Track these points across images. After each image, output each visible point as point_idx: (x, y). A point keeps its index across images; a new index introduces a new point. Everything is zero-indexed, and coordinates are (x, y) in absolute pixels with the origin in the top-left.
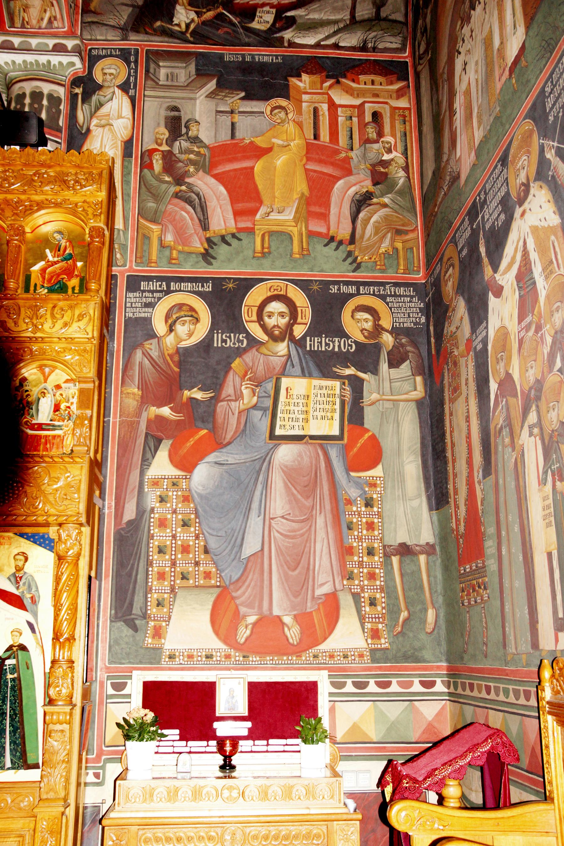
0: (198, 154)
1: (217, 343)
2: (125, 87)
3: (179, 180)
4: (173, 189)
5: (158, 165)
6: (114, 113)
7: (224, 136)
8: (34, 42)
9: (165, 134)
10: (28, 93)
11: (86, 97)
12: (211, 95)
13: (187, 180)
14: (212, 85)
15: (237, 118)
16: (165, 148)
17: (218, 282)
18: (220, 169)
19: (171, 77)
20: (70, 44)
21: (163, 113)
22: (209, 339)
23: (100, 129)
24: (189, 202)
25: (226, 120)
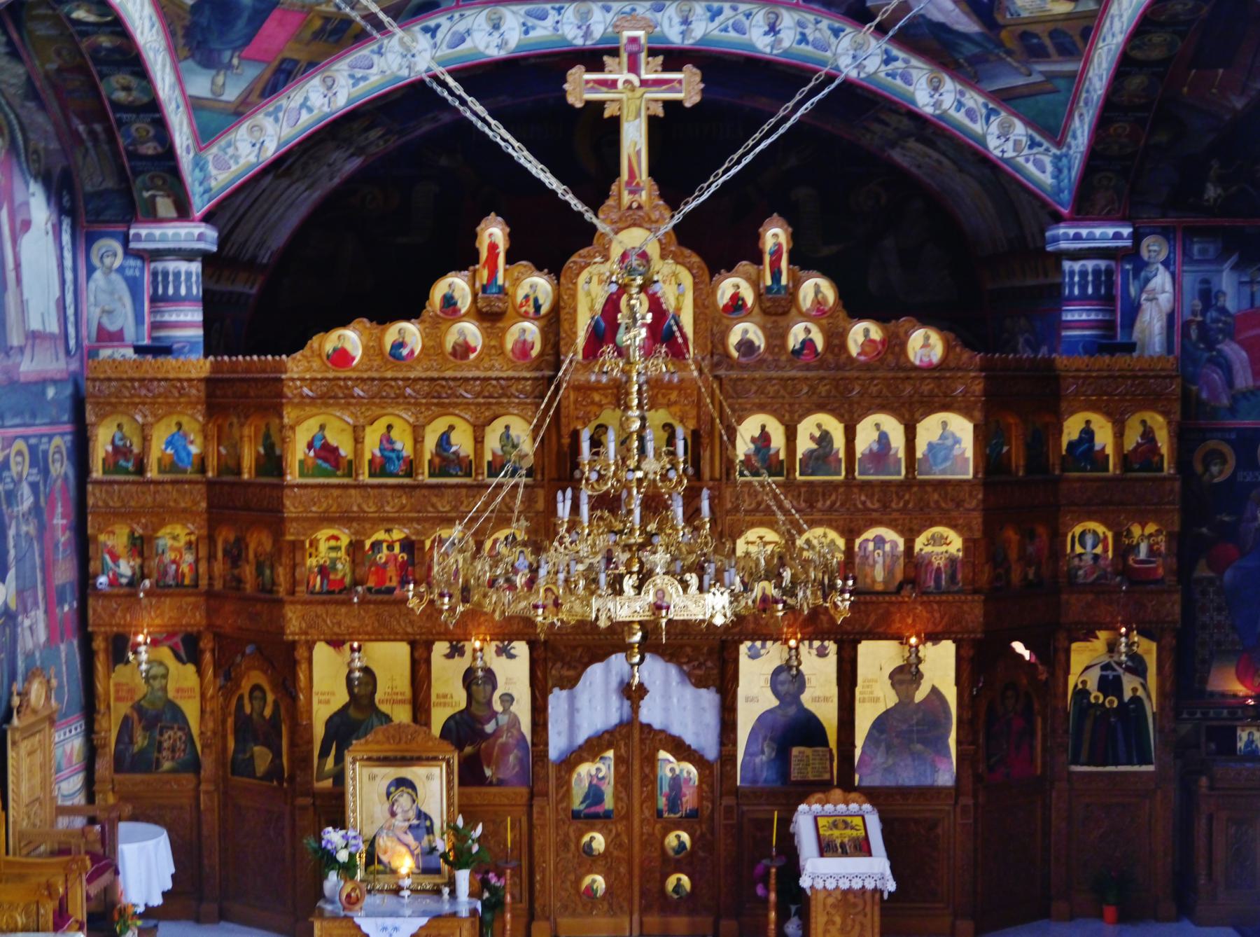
0: (1225, 323)
1: (1240, 479)
2: (1166, 263)
3: (1211, 346)
4: (1206, 355)
5: (1194, 334)
6: (1159, 288)
7: (1245, 304)
8: (1098, 232)
9: (1198, 305)
10: (1090, 270)
11: (1136, 275)
12: (1233, 268)
13: (1219, 346)
14: (1234, 259)
15: (1256, 288)
16: (1199, 318)
17: (1241, 432)
18: (1242, 337)
19: (1201, 252)
20: (1126, 231)
21: (1197, 286)
22: (1234, 475)
23: (1149, 304)
24: (1219, 365)
25: (1247, 290)
